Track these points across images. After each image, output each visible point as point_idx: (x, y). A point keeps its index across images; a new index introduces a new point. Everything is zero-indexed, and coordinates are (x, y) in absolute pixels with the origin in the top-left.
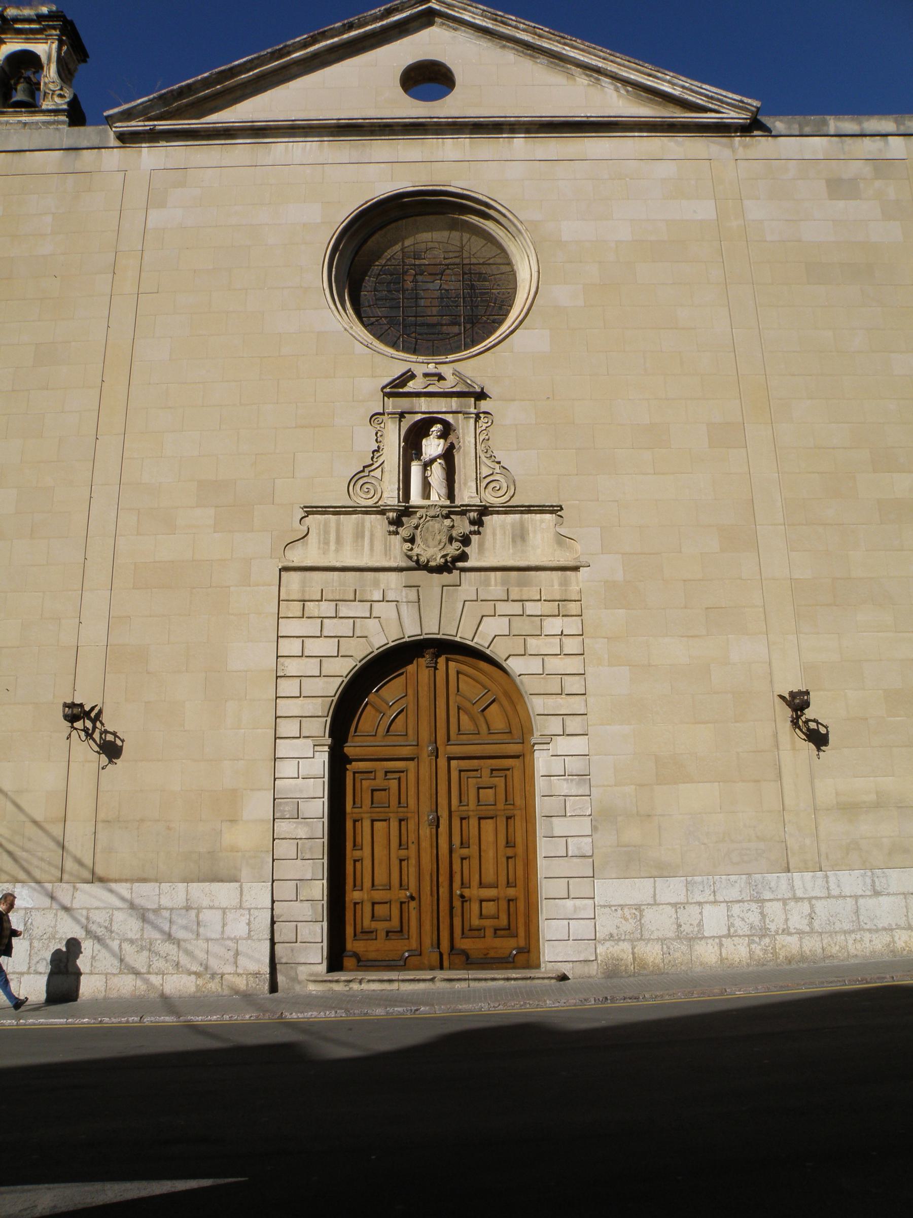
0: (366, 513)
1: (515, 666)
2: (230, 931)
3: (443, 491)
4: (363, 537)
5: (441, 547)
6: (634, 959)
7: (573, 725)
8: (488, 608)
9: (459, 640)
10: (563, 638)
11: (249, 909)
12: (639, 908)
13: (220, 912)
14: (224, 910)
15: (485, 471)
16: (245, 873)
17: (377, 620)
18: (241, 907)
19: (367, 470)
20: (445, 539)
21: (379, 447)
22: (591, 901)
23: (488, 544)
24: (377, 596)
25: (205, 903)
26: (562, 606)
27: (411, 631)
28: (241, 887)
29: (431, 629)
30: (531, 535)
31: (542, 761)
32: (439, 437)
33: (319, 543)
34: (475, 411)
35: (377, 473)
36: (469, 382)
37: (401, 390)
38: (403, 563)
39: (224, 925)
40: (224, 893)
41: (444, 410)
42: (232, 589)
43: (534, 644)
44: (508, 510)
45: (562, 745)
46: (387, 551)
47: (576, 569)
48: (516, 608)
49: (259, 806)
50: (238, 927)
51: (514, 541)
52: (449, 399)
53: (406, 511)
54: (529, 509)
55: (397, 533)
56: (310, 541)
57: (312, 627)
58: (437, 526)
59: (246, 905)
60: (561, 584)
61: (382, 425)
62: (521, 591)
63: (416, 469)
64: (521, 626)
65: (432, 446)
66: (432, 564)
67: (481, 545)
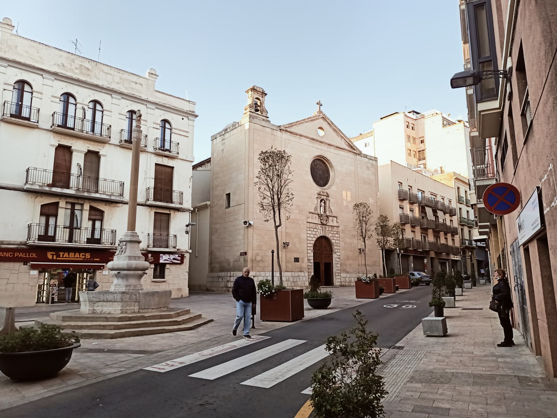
1: (333, 241)
7: (339, 251)
26: (337, 233)
31: (334, 256)
40: (302, 274)
50: (304, 280)
57: (310, 232)
64: (333, 235)
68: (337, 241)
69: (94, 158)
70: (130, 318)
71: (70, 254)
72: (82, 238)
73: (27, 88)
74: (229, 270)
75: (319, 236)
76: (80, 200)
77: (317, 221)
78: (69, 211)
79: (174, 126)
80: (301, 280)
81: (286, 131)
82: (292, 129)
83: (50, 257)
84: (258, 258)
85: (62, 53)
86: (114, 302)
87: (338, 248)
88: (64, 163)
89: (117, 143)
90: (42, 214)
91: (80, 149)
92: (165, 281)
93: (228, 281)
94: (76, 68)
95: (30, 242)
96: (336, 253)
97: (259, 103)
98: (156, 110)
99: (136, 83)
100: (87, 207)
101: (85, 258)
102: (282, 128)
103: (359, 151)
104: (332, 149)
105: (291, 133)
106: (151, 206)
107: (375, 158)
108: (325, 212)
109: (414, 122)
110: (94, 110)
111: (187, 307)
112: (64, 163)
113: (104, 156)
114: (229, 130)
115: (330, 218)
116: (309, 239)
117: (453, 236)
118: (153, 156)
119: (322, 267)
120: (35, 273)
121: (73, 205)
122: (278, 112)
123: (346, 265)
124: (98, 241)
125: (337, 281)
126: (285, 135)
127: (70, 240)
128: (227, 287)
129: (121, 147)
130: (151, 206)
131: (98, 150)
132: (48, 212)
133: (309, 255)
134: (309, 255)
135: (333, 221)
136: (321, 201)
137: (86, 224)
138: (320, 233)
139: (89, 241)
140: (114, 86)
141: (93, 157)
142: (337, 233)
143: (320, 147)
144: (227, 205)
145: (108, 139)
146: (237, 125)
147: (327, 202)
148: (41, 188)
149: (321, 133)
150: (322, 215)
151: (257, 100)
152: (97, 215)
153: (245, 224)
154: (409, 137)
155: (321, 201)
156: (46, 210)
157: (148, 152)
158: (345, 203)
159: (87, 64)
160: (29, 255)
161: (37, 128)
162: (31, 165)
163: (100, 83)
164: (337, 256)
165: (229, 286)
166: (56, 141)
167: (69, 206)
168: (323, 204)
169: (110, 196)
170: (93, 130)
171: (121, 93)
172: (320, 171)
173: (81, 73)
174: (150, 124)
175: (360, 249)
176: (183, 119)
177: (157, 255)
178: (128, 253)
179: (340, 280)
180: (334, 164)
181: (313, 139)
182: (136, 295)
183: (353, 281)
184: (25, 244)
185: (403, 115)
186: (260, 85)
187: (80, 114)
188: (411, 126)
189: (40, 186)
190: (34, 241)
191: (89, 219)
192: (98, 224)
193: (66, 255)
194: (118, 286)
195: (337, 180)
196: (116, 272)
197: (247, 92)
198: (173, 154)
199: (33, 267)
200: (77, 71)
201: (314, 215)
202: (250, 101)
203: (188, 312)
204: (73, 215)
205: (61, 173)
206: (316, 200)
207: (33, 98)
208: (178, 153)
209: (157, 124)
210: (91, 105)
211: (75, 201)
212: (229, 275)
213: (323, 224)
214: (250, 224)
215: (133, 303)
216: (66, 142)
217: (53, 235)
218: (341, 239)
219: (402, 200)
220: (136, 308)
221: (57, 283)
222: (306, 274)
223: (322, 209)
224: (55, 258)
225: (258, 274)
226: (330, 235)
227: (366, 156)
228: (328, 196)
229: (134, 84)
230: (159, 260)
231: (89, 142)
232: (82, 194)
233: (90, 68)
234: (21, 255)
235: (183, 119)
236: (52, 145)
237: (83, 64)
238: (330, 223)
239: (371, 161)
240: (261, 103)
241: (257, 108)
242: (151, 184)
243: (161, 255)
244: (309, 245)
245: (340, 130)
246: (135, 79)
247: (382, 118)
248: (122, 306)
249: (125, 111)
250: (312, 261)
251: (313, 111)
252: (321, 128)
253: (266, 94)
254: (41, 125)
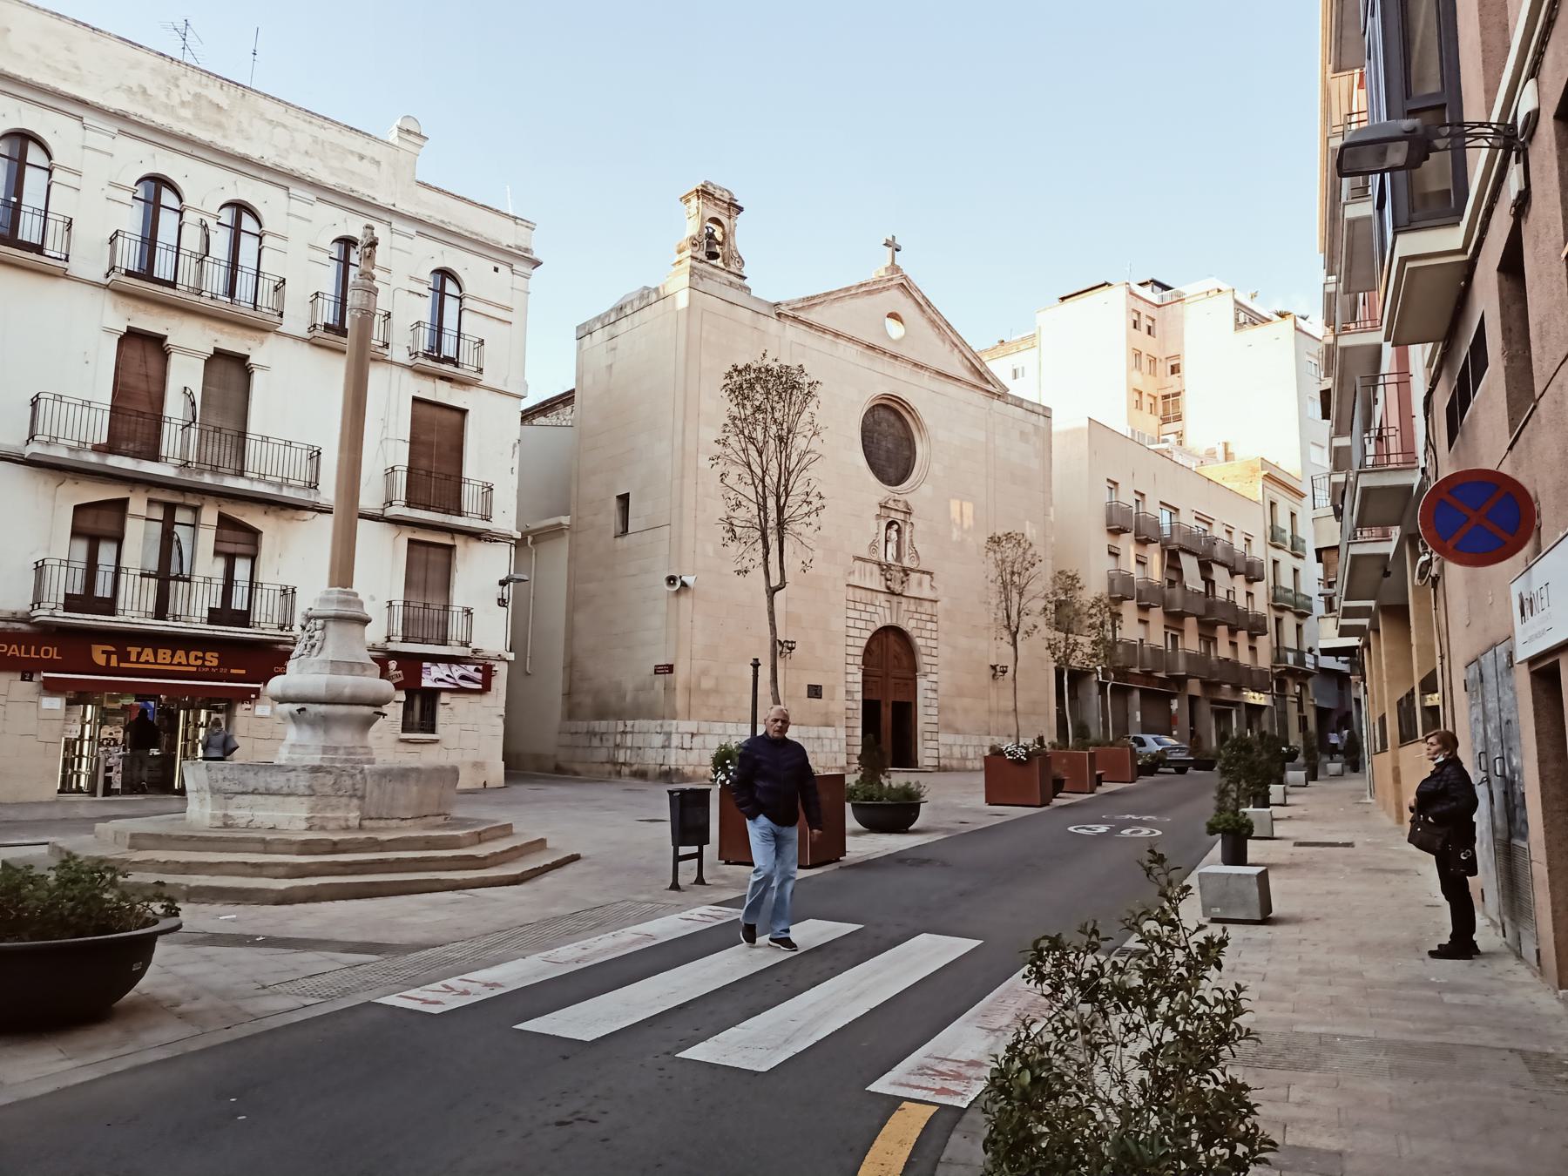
1: (919, 642)
26: (933, 618)
27: (888, 622)
31: (922, 683)
40: (829, 731)
45: (933, 678)
49: (841, 693)
50: (835, 748)
57: (856, 614)
64: (921, 624)
68: (932, 643)
69: (235, 374)
70: (335, 843)
71: (160, 651)
72: (194, 609)
73: (34, 155)
74: (620, 715)
75: (879, 625)
76: (189, 496)
77: (877, 582)
78: (157, 528)
79: (468, 289)
80: (827, 749)
81: (795, 318)
82: (812, 316)
83: (100, 659)
84: (707, 684)
85: (140, 54)
86: (289, 795)
87: (934, 660)
88: (143, 386)
89: (304, 333)
90: (76, 533)
91: (191, 345)
92: (436, 741)
93: (617, 746)
94: (183, 103)
95: (42, 614)
97: (718, 235)
98: (419, 239)
99: (362, 158)
100: (209, 516)
101: (203, 665)
102: (784, 309)
103: (1002, 386)
104: (925, 378)
105: (810, 325)
106: (397, 522)
107: (1045, 408)
108: (899, 557)
109: (1154, 313)
110: (237, 231)
111: (504, 818)
112: (143, 386)
113: (264, 368)
114: (628, 311)
115: (914, 576)
116: (852, 632)
117: (1252, 637)
118: (407, 376)
119: (887, 714)
120: (56, 703)
121: (170, 509)
122: (775, 265)
123: (954, 710)
124: (243, 618)
125: (926, 753)
126: (792, 332)
127: (161, 611)
128: (615, 763)
129: (314, 343)
130: (397, 522)
131: (246, 352)
132: (97, 527)
133: (850, 678)
134: (850, 678)
135: (920, 584)
136: (889, 525)
137: (208, 567)
138: (883, 617)
139: (215, 616)
140: (293, 163)
141: (230, 371)
142: (933, 618)
143: (889, 371)
144: (620, 529)
145: (277, 319)
146: (654, 297)
147: (907, 530)
148: (73, 456)
149: (895, 330)
150: (889, 566)
151: (714, 226)
152: (240, 542)
153: (669, 584)
154: (1138, 354)
155: (889, 525)
156: (88, 523)
157: (392, 362)
158: (956, 535)
159: (215, 93)
160: (38, 652)
161: (66, 276)
162: (47, 387)
163: (254, 153)
164: (929, 685)
165: (621, 760)
166: (122, 317)
167: (158, 513)
168: (894, 535)
169: (280, 486)
170: (231, 292)
171: (314, 185)
172: (890, 441)
173: (197, 117)
174: (400, 280)
175: (994, 667)
176: (496, 270)
177: (412, 665)
178: (329, 653)
179: (935, 753)
180: (927, 420)
181: (871, 347)
182: (352, 776)
183: (971, 755)
184: (26, 619)
185: (1123, 291)
186: (723, 181)
187: (192, 241)
188: (1145, 323)
189: (70, 449)
190: (52, 611)
191: (217, 553)
192: (242, 569)
193: (148, 654)
194: (298, 750)
195: (936, 468)
196: (294, 707)
197: (686, 199)
198: (467, 371)
199: (51, 688)
200: (187, 113)
201: (869, 566)
202: (692, 228)
203: (507, 831)
204: (168, 538)
205: (135, 414)
206: (873, 523)
207: (54, 187)
208: (480, 371)
209: (420, 281)
210: (227, 216)
211: (176, 498)
212: (621, 728)
213: (893, 593)
214: (684, 584)
215: (344, 800)
216: (151, 321)
217: (108, 595)
218: (941, 636)
219: (1116, 532)
220: (352, 815)
221: (121, 736)
222: (842, 733)
223: (892, 548)
224: (114, 663)
225: (704, 727)
226: (912, 623)
227: (1019, 403)
228: (908, 513)
229: (356, 159)
230: (420, 678)
231: (218, 326)
232: (196, 478)
233: (224, 103)
234: (14, 650)
235: (496, 270)
236: (109, 331)
237: (205, 92)
238: (912, 590)
239: (1034, 417)
240: (724, 234)
241: (712, 248)
242: (401, 457)
243: (425, 665)
244: (851, 650)
245: (948, 325)
246: (358, 143)
247: (1063, 299)
248: (312, 809)
249: (326, 240)
250: (859, 696)
251: (875, 266)
252: (894, 316)
253: (741, 209)
254: (74, 267)
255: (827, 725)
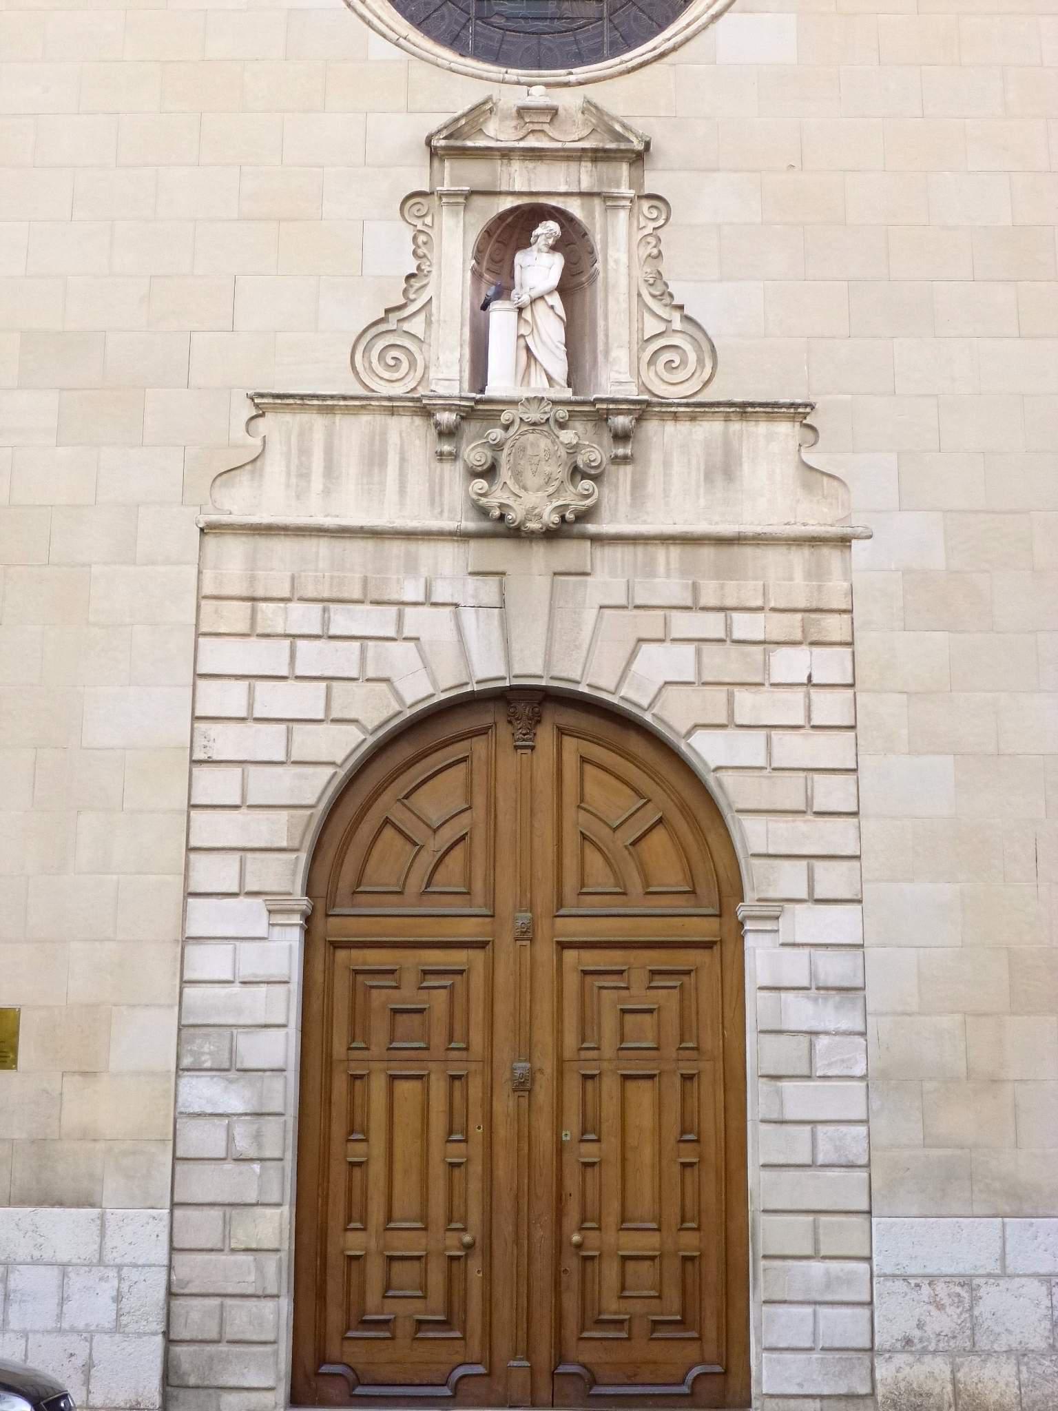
0: (392, 411)
1: (708, 750)
2: (76, 1315)
3: (559, 369)
4: (383, 464)
5: (551, 490)
6: (956, 1393)
7: (831, 879)
8: (650, 624)
9: (586, 690)
10: (813, 691)
11: (119, 1267)
12: (966, 1281)
13: (55, 1271)
14: (64, 1268)
15: (652, 327)
16: (112, 1186)
17: (412, 644)
18: (101, 1262)
19: (393, 317)
20: (561, 473)
21: (419, 268)
22: (863, 1267)
23: (654, 485)
24: (412, 591)
25: (22, 1253)
26: (811, 622)
27: (488, 667)
28: (102, 1218)
29: (531, 666)
30: (746, 466)
31: (762, 958)
32: (554, 248)
33: (288, 474)
34: (631, 193)
35: (416, 326)
36: (618, 128)
37: (469, 143)
38: (471, 525)
39: (63, 1300)
40: (64, 1230)
41: (563, 189)
42: (96, 569)
43: (748, 705)
44: (698, 410)
45: (806, 923)
46: (435, 496)
47: (844, 541)
48: (711, 625)
49: (146, 1040)
51: (708, 477)
52: (573, 166)
53: (478, 410)
54: (744, 410)
55: (454, 457)
56: (268, 469)
57: (271, 657)
58: (544, 443)
59: (109, 1257)
60: (809, 576)
61: (428, 220)
62: (722, 587)
63: (501, 318)
65: (539, 268)
66: (533, 525)
67: (638, 486)
96: (774, 909)
147: (617, 244)
164: (795, 969)
179: (846, 1326)
201: (353, 431)
213: (506, 530)
222: (140, 1235)
255: (47, 1197)
